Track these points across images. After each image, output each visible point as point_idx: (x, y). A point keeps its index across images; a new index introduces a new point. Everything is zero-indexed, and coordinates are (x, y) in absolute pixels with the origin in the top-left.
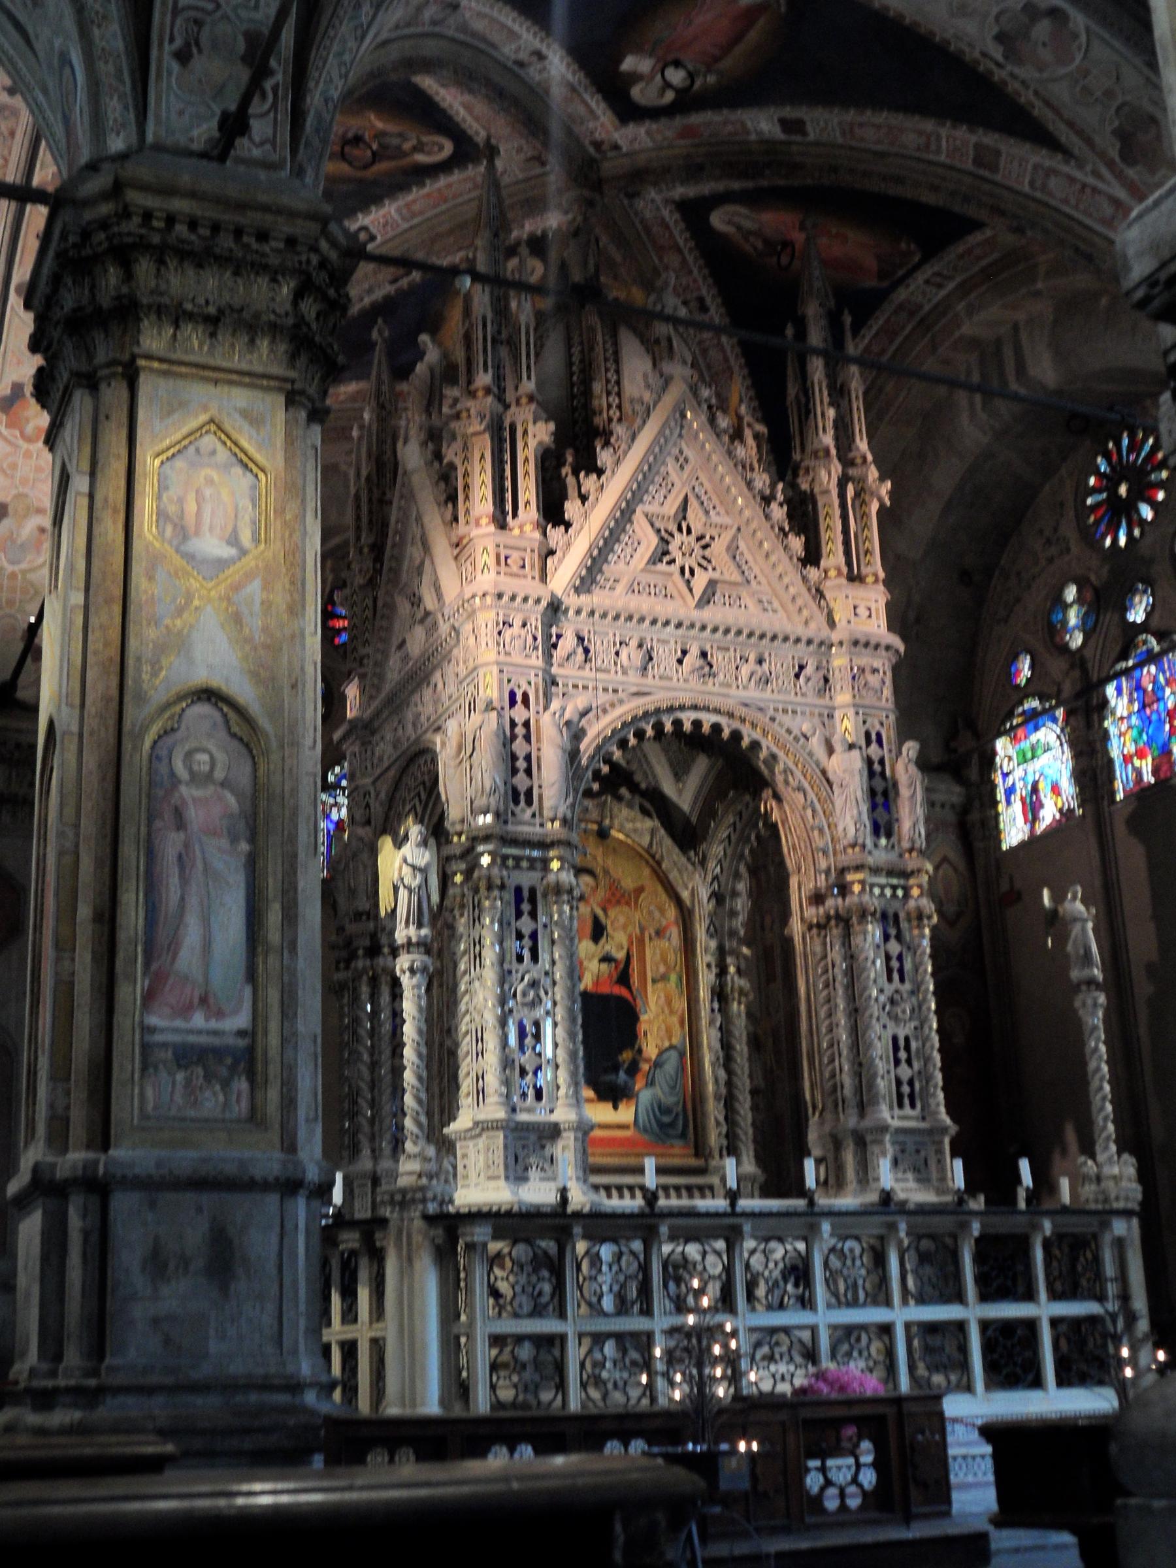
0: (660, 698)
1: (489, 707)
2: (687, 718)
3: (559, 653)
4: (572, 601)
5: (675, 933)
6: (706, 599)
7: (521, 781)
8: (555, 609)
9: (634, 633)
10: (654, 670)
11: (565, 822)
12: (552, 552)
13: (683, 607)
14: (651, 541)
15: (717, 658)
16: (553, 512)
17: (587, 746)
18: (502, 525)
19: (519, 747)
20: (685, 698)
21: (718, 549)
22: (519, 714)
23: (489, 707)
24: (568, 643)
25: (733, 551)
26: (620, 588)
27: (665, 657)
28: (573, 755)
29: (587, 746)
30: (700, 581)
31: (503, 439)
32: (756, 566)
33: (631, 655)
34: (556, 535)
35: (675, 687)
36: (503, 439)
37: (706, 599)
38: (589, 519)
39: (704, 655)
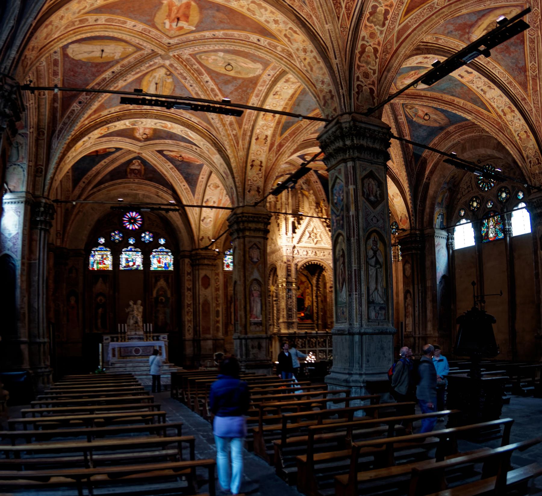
0: (309, 259)
1: (285, 263)
2: (313, 262)
3: (295, 253)
4: (296, 245)
5: (310, 288)
6: (316, 243)
7: (289, 273)
8: (294, 247)
9: (305, 249)
10: (309, 255)
11: (296, 279)
12: (293, 237)
13: (313, 245)
14: (308, 235)
15: (317, 252)
16: (294, 232)
17: (298, 267)
18: (286, 234)
19: (289, 268)
20: (312, 259)
21: (318, 236)
22: (289, 263)
23: (285, 263)
24: (296, 252)
25: (320, 236)
26: (304, 242)
27: (310, 252)
28: (296, 269)
29: (298, 267)
30: (315, 240)
31: (286, 220)
32: (324, 238)
33: (305, 253)
34: (294, 235)
35: (311, 256)
36: (286, 220)
37: (316, 243)
38: (299, 231)
39: (315, 252)
